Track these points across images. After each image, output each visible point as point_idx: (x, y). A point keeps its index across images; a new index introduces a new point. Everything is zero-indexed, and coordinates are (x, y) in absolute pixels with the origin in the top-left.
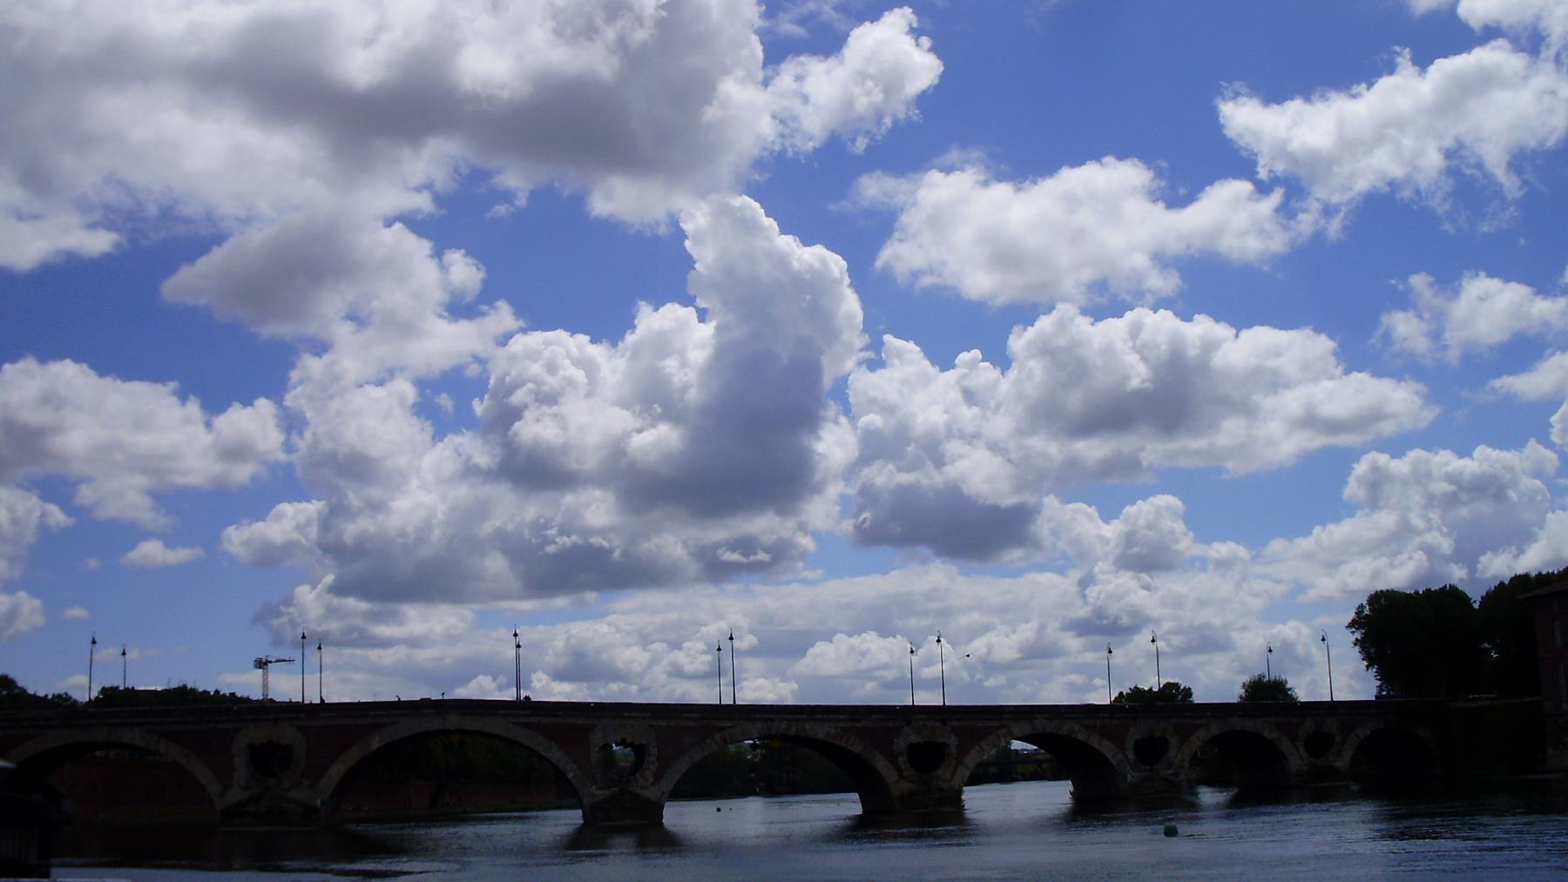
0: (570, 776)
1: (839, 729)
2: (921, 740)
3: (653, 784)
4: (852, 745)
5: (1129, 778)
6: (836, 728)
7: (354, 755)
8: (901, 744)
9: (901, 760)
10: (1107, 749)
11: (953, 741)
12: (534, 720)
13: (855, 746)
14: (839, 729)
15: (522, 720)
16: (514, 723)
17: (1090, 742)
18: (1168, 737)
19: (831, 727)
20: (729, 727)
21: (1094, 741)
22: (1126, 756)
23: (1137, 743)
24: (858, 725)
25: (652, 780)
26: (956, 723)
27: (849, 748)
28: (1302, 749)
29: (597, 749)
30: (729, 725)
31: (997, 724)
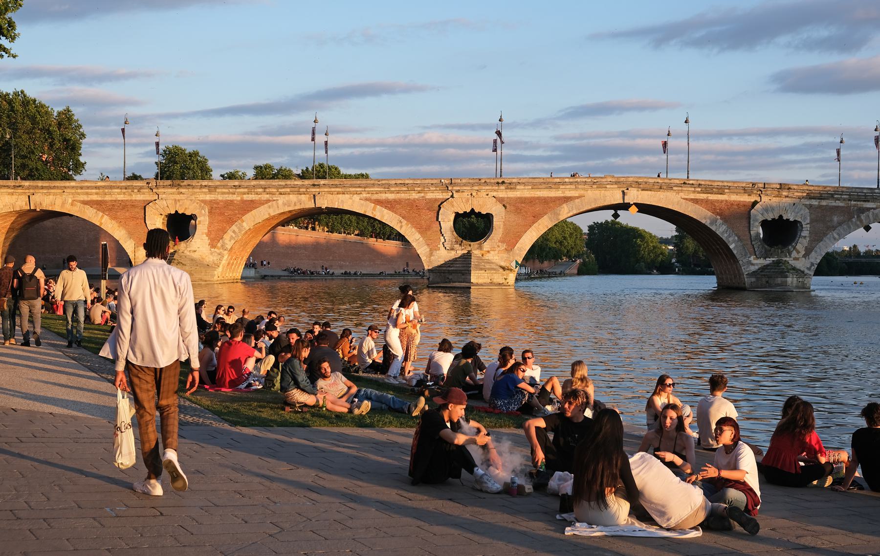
0: (732, 247)
3: (804, 256)
12: (703, 196)
15: (692, 196)
16: (686, 199)
25: (803, 253)
30: (874, 206)
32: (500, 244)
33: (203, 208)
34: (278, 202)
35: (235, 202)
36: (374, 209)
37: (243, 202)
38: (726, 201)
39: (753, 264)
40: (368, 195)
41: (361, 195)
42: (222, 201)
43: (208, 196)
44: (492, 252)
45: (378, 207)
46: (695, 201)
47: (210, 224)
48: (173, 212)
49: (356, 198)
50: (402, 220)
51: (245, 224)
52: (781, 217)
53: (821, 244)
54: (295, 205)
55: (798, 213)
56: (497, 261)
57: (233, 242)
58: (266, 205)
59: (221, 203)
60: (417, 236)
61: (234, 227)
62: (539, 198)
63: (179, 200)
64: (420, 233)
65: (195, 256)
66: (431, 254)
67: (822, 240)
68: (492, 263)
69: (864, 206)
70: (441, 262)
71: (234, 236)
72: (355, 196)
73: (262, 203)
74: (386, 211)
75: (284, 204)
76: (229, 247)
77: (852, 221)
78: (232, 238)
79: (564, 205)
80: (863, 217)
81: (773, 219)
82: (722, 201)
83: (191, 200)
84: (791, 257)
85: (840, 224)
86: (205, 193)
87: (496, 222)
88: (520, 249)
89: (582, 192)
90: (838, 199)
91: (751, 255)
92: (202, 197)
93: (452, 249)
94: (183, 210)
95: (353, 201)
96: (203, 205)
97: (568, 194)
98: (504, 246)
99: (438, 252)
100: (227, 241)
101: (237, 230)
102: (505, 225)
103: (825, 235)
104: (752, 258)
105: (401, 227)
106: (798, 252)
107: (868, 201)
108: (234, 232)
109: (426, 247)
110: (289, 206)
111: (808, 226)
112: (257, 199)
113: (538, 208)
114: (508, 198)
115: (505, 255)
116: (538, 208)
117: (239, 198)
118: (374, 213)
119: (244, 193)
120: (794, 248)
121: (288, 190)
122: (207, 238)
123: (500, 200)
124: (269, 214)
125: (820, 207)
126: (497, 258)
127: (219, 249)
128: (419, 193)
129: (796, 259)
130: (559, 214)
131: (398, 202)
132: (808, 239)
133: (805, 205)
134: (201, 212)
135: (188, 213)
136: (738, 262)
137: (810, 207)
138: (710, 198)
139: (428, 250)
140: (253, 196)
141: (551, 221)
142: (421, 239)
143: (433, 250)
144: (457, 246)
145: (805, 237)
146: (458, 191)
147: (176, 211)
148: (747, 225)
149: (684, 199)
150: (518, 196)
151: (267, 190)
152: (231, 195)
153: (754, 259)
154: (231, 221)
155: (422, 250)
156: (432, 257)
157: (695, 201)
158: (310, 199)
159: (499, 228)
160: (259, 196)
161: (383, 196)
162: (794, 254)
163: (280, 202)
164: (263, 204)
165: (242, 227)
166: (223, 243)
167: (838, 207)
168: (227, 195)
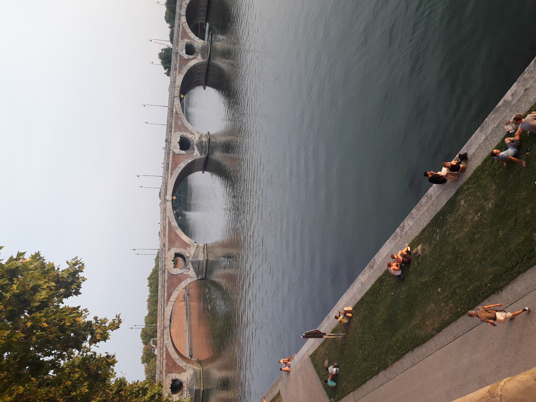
0: (190, 161)
1: (179, 75)
3: (194, 135)
4: (184, 71)
7: (179, 232)
8: (186, 56)
9: (191, 57)
11: (186, 40)
12: (170, 171)
14: (179, 75)
15: (169, 175)
16: (170, 178)
20: (176, 109)
25: (193, 135)
29: (181, 151)
30: (175, 109)
32: (187, 249)
33: (169, 376)
34: (166, 343)
35: (166, 362)
36: (171, 301)
37: (166, 359)
38: (172, 162)
39: (197, 154)
40: (165, 304)
41: (165, 307)
42: (166, 368)
43: (163, 374)
44: (191, 253)
45: (170, 300)
46: (172, 174)
47: (175, 373)
48: (170, 390)
49: (166, 309)
50: (176, 289)
51: (176, 357)
52: (178, 143)
53: (189, 129)
54: (168, 335)
55: (177, 136)
56: (194, 251)
57: (183, 362)
58: (168, 348)
59: (167, 368)
60: (183, 283)
61: (177, 362)
62: (168, 234)
63: (165, 387)
64: (181, 282)
65: (189, 379)
66: (191, 277)
67: (188, 128)
68: (195, 252)
70: (194, 273)
71: (181, 362)
72: (165, 310)
73: (167, 350)
74: (172, 297)
75: (168, 340)
76: (186, 364)
77: (181, 117)
78: (182, 363)
79: (172, 224)
80: (179, 113)
81: (179, 145)
82: (172, 164)
83: (165, 382)
84: (194, 140)
85: (182, 121)
86: (162, 376)
87: (178, 251)
88: (190, 242)
89: (167, 217)
90: (172, 121)
91: (193, 154)
92: (164, 377)
93: (189, 269)
94: (169, 385)
95: (167, 310)
96: (167, 376)
97: (167, 222)
98: (188, 248)
99: (190, 274)
100: (183, 365)
101: (179, 361)
102: (179, 248)
103: (186, 127)
104: (195, 154)
105: (179, 290)
106: (192, 137)
108: (179, 362)
109: (187, 279)
110: (168, 338)
111: (182, 133)
112: (165, 352)
113: (173, 235)
114: (168, 247)
115: (192, 247)
116: (173, 235)
117: (165, 360)
118: (173, 301)
119: (163, 358)
120: (191, 138)
121: (162, 339)
122: (182, 374)
123: (169, 249)
124: (172, 347)
125: (175, 128)
126: (193, 251)
127: (186, 368)
128: (165, 283)
129: (195, 138)
130: (176, 226)
131: (168, 291)
132: (187, 133)
133: (174, 133)
134: (171, 377)
135: (171, 383)
136: (196, 159)
137: (175, 132)
138: (170, 168)
139: (189, 278)
140: (164, 354)
141: (178, 229)
142: (184, 281)
143: (188, 276)
144: (188, 267)
145: (186, 134)
146: (165, 267)
147: (170, 388)
148: (181, 155)
149: (170, 178)
150: (167, 242)
151: (162, 348)
152: (163, 364)
153: (195, 153)
154: (175, 364)
155: (189, 281)
156: (192, 277)
157: (172, 174)
158: (166, 329)
159: (180, 250)
160: (164, 351)
161: (166, 298)
162: (193, 139)
163: (167, 342)
164: (168, 350)
165: (177, 358)
166: (184, 366)
167: (175, 122)
168: (163, 366)
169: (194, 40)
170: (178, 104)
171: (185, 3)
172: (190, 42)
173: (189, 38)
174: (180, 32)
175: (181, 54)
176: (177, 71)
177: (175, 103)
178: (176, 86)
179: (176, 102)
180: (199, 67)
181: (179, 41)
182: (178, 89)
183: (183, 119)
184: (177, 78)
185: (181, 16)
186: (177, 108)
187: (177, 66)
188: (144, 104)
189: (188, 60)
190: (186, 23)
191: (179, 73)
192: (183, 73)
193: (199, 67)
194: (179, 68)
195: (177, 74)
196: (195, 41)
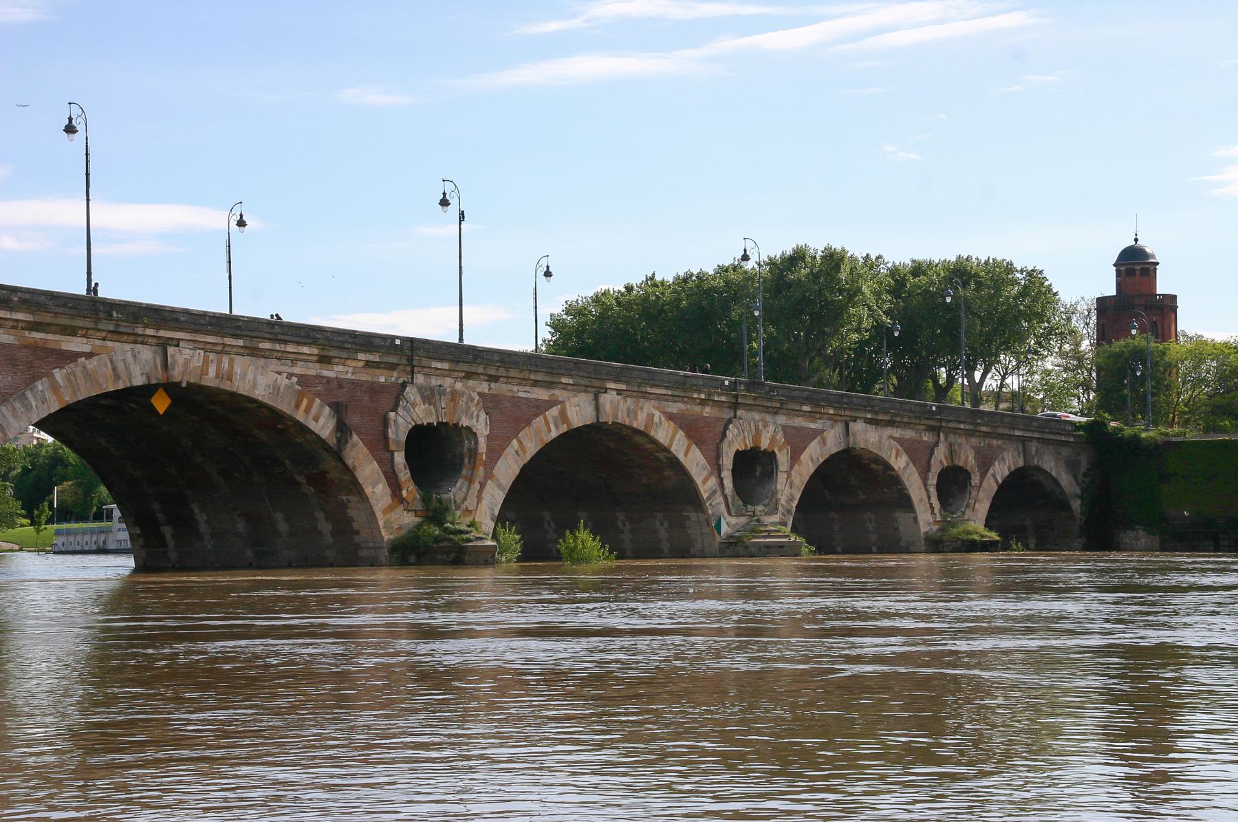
1: (295, 379)
2: (433, 420)
4: (316, 419)
5: (724, 529)
6: (290, 376)
8: (400, 426)
9: (400, 458)
10: (694, 462)
13: (322, 421)
17: (673, 449)
18: (776, 450)
19: (280, 373)
20: (89, 355)
21: (679, 445)
22: (722, 484)
23: (738, 453)
24: (329, 373)
26: (484, 387)
27: (312, 425)
28: (933, 490)
30: (87, 348)
31: (541, 394)
69: (65, 347)
107: (72, 332)
169: (486, 479)
170: (117, 377)
171: (653, 415)
172: (474, 453)
173: (496, 452)
174: (515, 388)
175: (411, 393)
176: (313, 370)
177: (122, 351)
178: (225, 360)
179: (129, 355)
180: (325, 527)
181: (471, 383)
182: (212, 372)
183: (18, 405)
184: (274, 365)
185: (591, 396)
186: (92, 364)
187: (340, 368)
188: (97, 131)
189: (380, 446)
190: (564, 429)
191: (303, 380)
192: (307, 411)
193: (325, 527)
194: (329, 380)
195: (296, 370)
196: (483, 485)
